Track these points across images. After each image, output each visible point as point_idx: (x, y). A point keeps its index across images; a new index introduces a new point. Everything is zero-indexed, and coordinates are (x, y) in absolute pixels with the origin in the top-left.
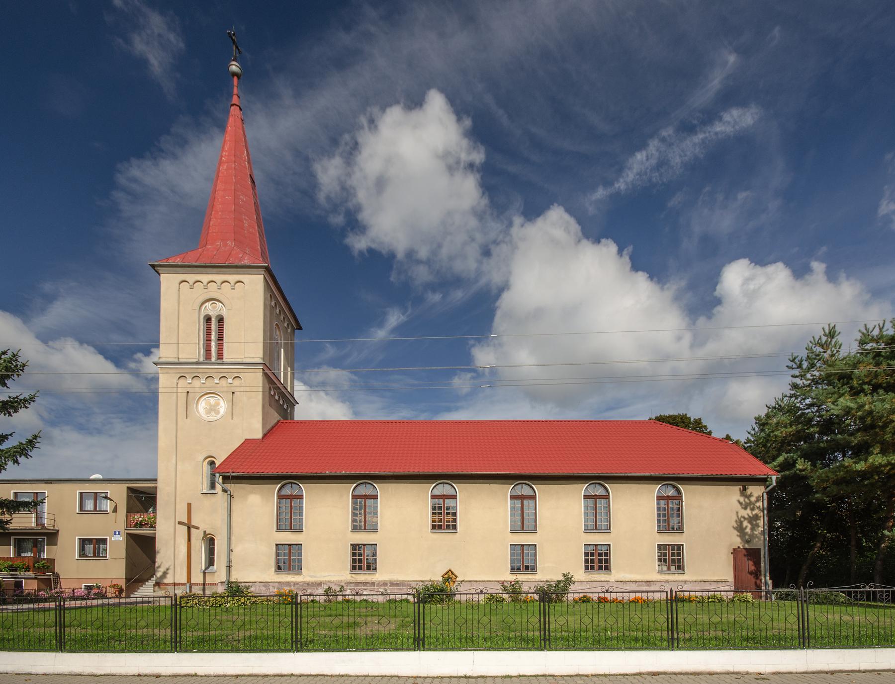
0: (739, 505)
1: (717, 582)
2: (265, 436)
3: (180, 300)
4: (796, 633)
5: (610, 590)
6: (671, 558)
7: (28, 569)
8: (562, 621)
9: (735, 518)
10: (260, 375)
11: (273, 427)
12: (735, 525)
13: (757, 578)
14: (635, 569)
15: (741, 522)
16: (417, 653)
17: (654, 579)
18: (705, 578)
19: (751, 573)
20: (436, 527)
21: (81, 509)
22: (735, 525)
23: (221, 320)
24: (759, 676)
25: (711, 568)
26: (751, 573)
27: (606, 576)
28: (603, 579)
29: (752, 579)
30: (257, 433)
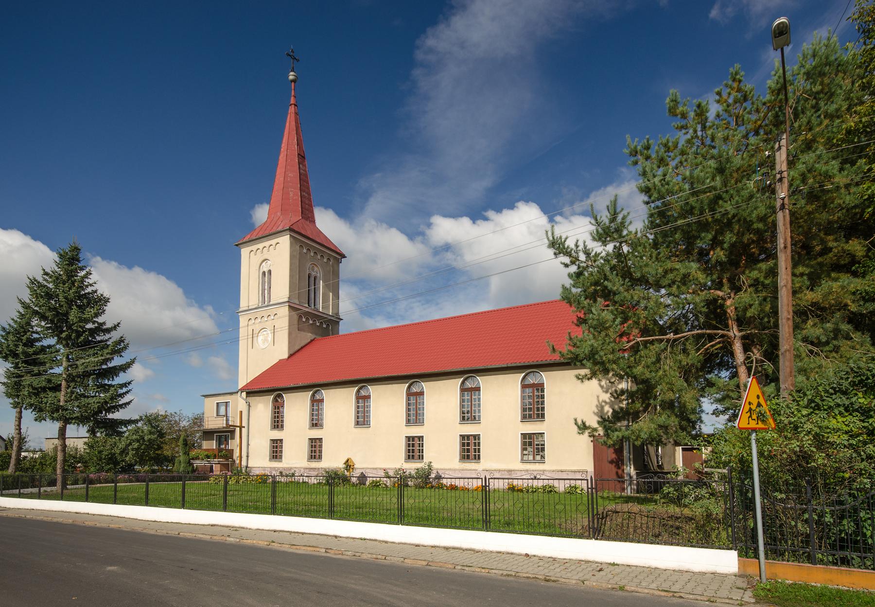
0: (599, 388)
1: (575, 472)
2: (291, 356)
3: (250, 259)
4: (480, 517)
5: (538, 477)
6: (533, 445)
7: (215, 457)
8: (411, 501)
9: (596, 403)
10: (287, 308)
11: (302, 348)
12: (596, 411)
13: (619, 468)
14: (501, 459)
15: (602, 407)
16: (182, 510)
17: (516, 468)
18: (563, 468)
19: (611, 462)
20: (357, 423)
21: (218, 415)
22: (596, 411)
23: (270, 271)
24: (840, 594)
25: (572, 457)
26: (611, 462)
27: (476, 465)
28: (473, 468)
29: (613, 467)
30: (286, 356)
